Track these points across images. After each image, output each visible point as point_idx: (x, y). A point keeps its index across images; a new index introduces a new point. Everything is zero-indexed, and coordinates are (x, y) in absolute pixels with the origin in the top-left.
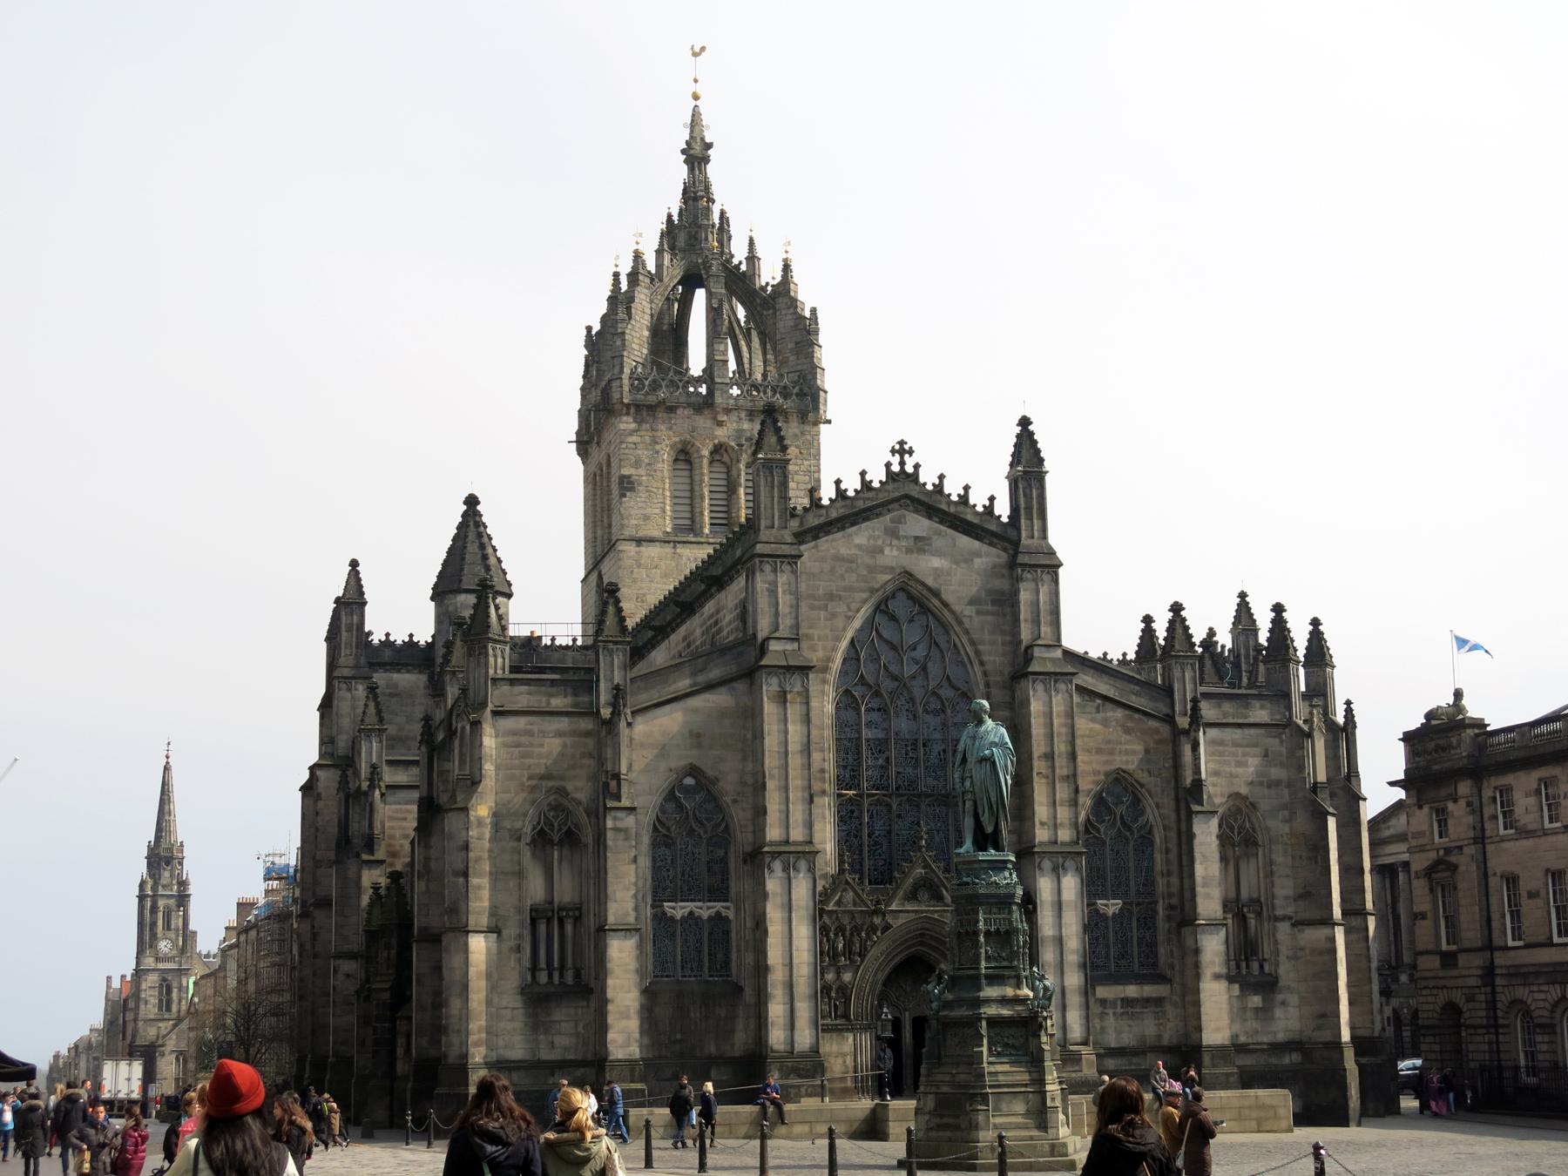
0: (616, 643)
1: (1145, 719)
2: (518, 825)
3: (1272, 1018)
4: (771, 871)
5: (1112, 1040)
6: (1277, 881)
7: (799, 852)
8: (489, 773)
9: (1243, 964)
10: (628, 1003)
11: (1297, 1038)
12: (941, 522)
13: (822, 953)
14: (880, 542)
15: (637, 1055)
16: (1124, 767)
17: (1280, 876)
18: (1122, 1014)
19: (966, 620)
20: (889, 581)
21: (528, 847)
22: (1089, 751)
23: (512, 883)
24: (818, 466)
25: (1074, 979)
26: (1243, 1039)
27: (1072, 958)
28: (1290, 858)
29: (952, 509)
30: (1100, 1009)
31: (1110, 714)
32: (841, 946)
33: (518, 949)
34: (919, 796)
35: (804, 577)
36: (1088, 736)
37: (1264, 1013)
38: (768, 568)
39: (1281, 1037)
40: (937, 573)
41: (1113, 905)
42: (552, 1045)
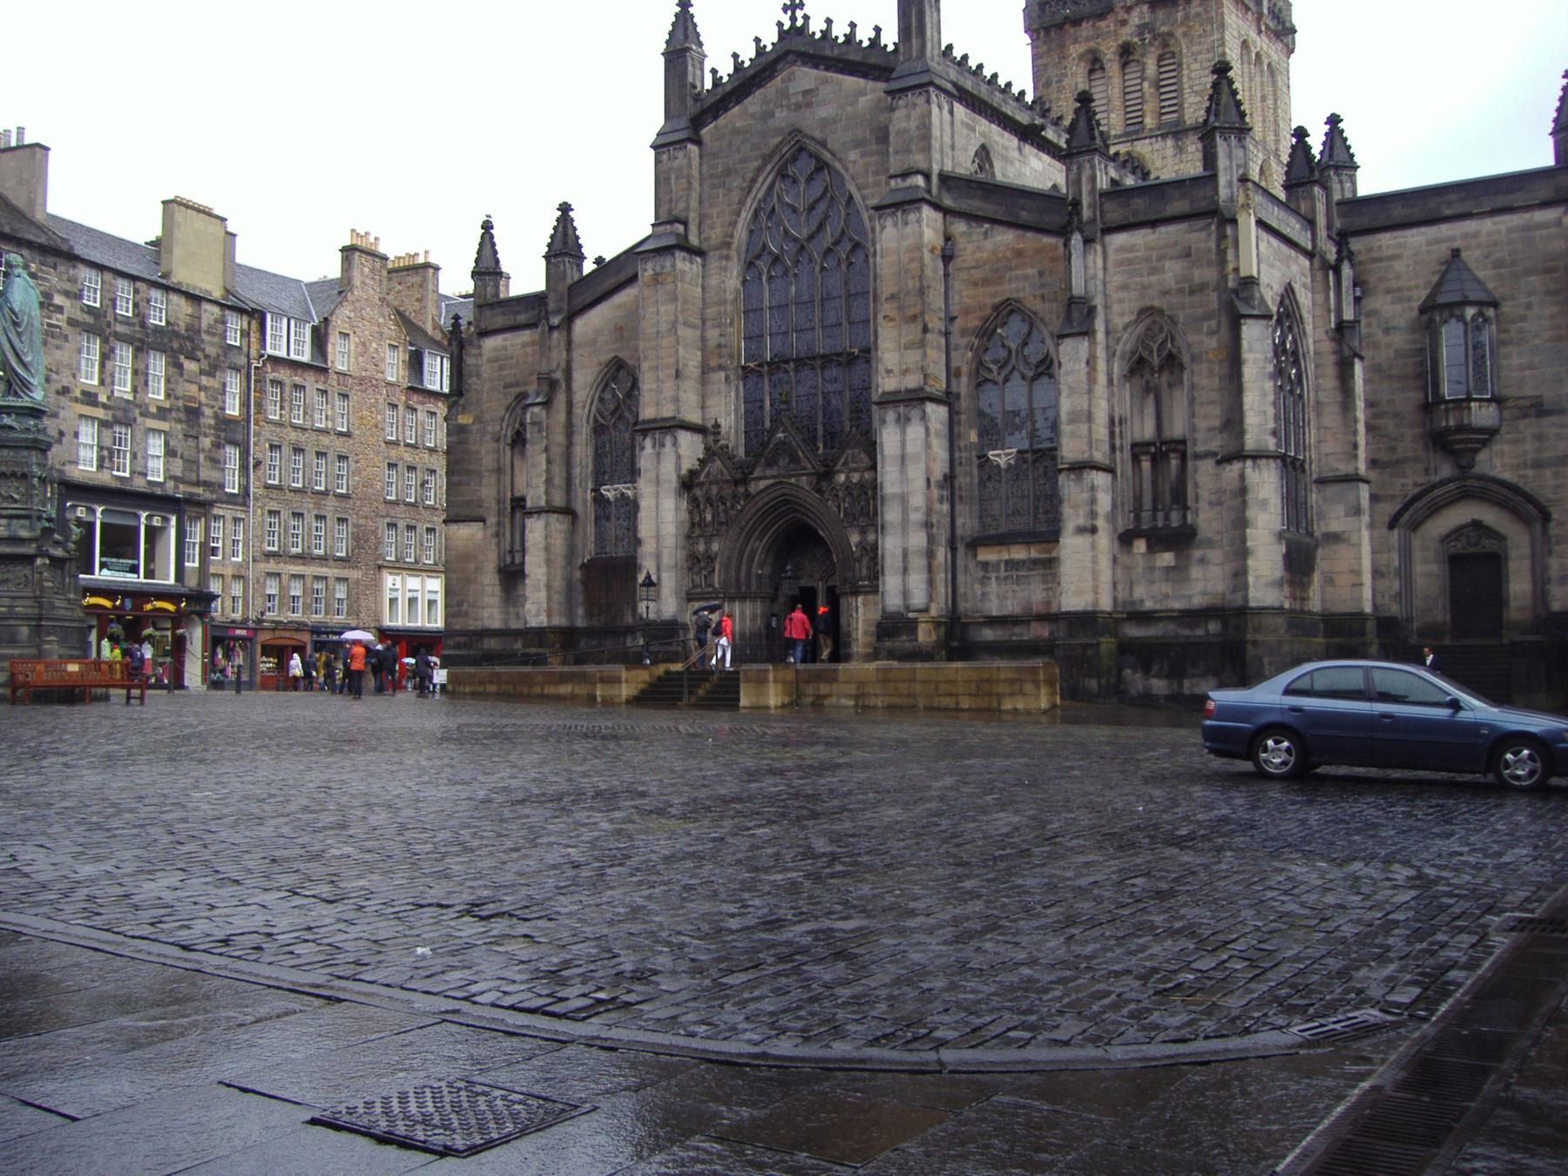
0: (556, 256)
1: (1040, 236)
2: (498, 428)
3: (1187, 579)
4: (643, 449)
5: (994, 608)
6: (1199, 410)
7: (661, 428)
8: (474, 387)
9: (1160, 515)
10: (540, 577)
11: (1218, 602)
12: (827, 69)
13: (693, 525)
14: (771, 106)
15: (545, 625)
16: (1014, 296)
17: (1202, 404)
18: (1006, 578)
19: (850, 165)
20: (781, 142)
21: (508, 448)
22: (976, 284)
23: (493, 479)
24: (1222, 38)
25: (918, 540)
26: (1149, 605)
27: (916, 517)
28: (1216, 380)
29: (836, 52)
30: (981, 574)
31: (999, 238)
32: (709, 517)
33: (497, 534)
34: (814, 358)
35: (705, 159)
36: (974, 268)
37: (1177, 573)
38: (665, 157)
39: (1197, 602)
40: (824, 123)
41: (1007, 455)
42: (518, 616)
